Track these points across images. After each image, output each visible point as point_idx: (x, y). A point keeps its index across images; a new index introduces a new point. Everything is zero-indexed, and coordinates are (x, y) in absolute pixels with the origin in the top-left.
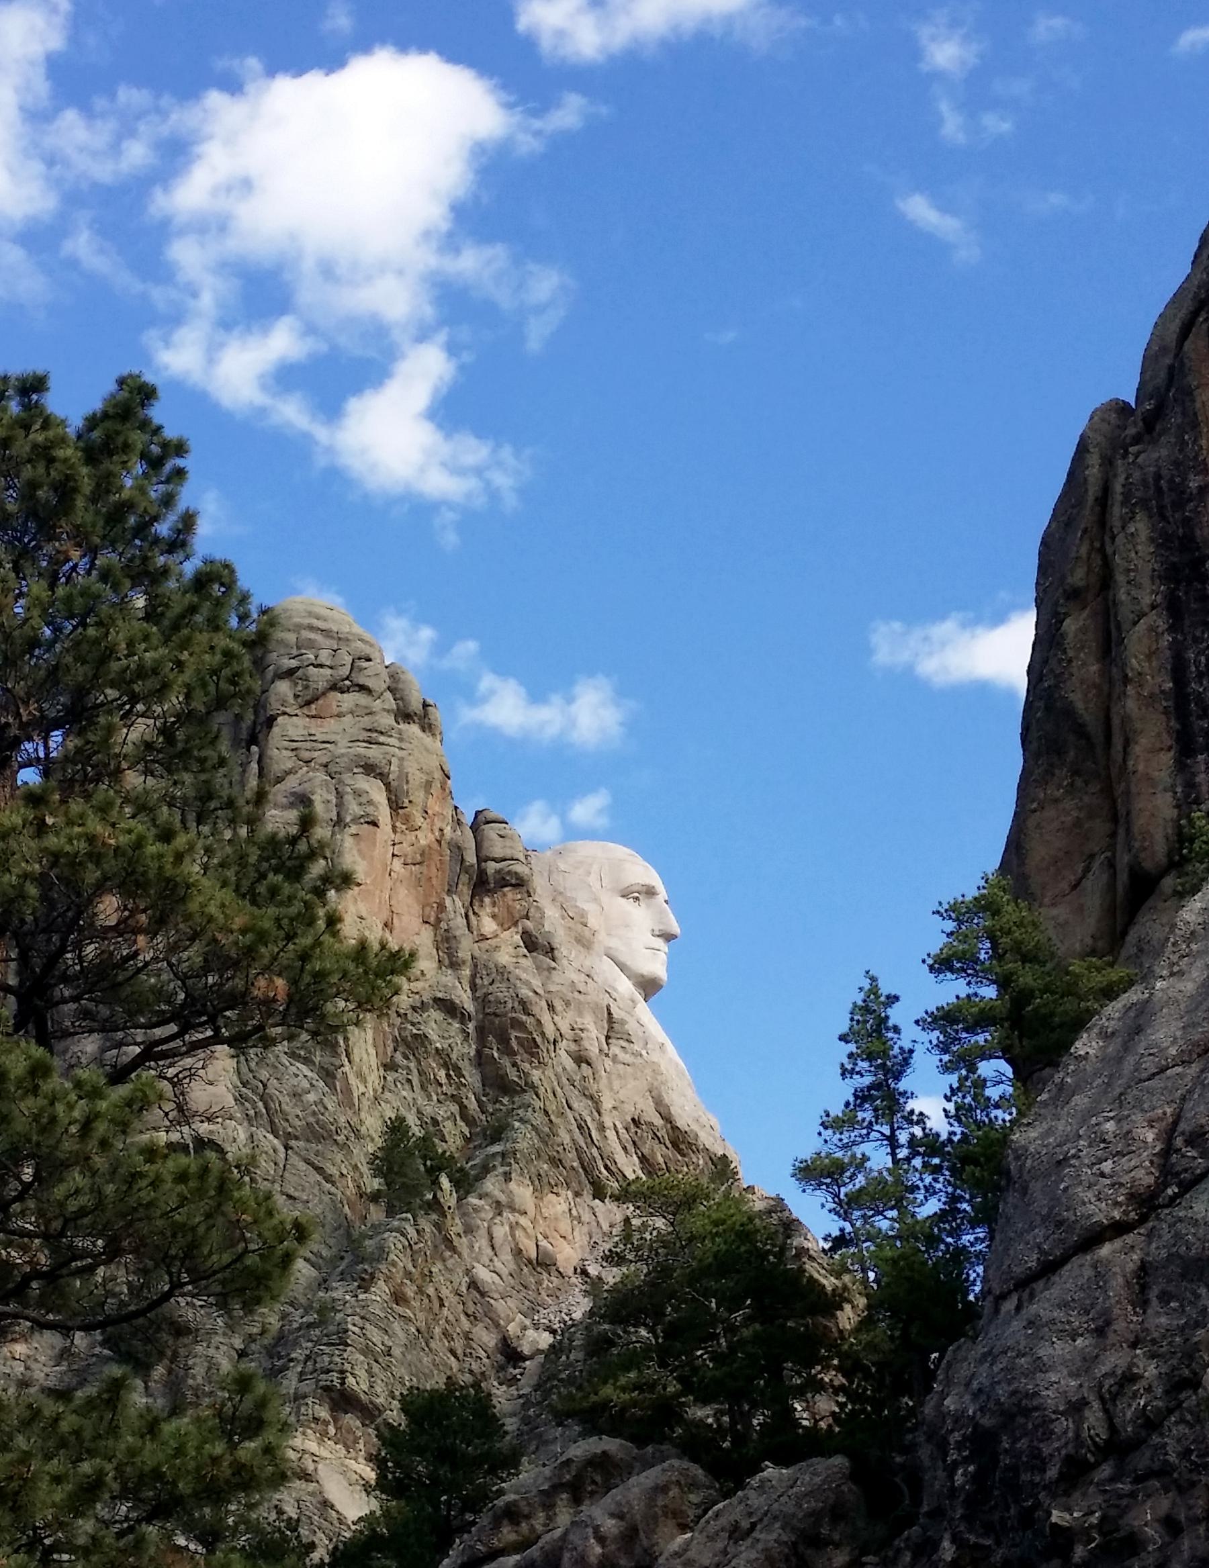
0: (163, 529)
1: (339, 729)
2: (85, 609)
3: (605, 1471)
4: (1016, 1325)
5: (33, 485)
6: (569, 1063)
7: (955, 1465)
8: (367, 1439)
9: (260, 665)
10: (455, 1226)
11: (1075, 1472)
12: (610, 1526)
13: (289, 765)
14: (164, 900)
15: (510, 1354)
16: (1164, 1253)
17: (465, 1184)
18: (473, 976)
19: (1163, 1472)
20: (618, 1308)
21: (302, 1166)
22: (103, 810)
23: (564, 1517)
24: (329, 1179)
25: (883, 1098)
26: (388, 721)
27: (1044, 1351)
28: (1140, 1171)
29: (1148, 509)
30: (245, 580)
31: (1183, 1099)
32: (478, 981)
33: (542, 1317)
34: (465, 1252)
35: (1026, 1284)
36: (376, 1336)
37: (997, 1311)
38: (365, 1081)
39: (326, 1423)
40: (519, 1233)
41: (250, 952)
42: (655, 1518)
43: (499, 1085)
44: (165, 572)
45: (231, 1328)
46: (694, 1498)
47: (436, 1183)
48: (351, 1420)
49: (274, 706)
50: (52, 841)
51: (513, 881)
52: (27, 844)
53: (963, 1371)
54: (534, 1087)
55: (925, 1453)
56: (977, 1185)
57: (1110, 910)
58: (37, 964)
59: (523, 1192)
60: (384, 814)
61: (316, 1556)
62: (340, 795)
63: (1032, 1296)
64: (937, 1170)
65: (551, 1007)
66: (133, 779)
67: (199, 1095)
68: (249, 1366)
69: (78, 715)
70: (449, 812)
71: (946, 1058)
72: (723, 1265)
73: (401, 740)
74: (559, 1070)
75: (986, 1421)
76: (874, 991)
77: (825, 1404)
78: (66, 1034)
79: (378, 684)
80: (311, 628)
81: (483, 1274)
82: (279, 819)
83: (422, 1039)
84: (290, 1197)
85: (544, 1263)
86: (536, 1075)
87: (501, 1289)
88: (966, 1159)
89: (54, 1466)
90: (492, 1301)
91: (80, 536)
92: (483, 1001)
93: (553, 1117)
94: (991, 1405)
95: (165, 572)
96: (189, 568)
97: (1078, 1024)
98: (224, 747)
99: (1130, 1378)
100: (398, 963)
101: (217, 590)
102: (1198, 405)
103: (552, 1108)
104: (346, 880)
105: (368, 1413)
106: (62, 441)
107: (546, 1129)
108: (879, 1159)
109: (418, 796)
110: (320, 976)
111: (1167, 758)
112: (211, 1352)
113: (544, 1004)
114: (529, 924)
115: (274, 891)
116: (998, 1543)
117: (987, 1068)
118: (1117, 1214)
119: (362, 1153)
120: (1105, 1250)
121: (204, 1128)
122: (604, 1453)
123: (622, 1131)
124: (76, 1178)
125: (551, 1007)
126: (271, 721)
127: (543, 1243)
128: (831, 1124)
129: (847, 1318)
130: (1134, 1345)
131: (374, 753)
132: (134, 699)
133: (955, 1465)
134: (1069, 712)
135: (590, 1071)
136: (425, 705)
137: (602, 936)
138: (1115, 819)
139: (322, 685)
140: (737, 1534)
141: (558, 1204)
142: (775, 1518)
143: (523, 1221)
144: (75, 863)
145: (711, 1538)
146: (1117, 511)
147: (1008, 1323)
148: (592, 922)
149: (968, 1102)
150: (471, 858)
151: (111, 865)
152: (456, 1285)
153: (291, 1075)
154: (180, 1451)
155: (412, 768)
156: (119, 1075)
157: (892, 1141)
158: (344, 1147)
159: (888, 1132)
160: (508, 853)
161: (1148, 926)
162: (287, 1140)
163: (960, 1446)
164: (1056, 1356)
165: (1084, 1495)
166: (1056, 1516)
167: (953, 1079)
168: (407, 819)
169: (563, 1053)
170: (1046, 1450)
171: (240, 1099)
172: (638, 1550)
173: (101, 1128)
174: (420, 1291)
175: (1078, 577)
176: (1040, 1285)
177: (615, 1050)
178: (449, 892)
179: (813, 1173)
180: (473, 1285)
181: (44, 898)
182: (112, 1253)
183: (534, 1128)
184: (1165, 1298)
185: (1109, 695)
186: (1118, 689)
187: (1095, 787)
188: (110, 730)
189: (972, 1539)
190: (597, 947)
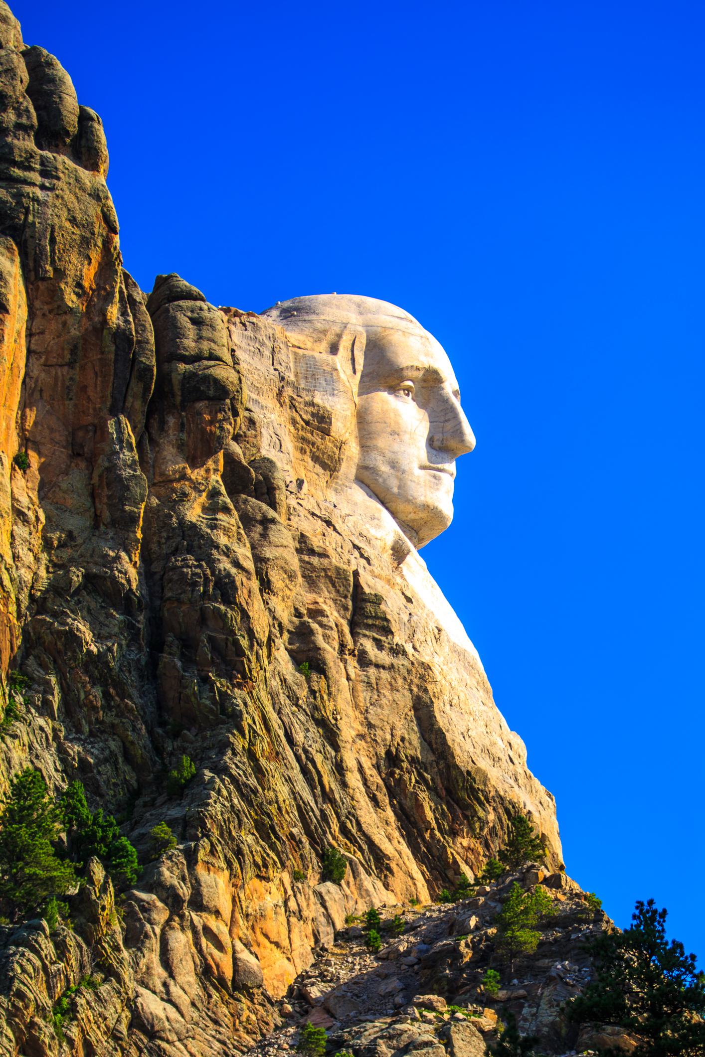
32: (154, 547)
34: (127, 974)
51: (211, 393)
73: (44, 174)
74: (275, 683)
87: (176, 1026)
90: (164, 1045)
93: (263, 762)
107: (253, 782)
113: (255, 584)
123: (370, 772)
125: (266, 586)
127: (244, 955)
135: (323, 683)
152: (111, 1023)
178: (114, 412)
183: (234, 780)
190: (348, 469)
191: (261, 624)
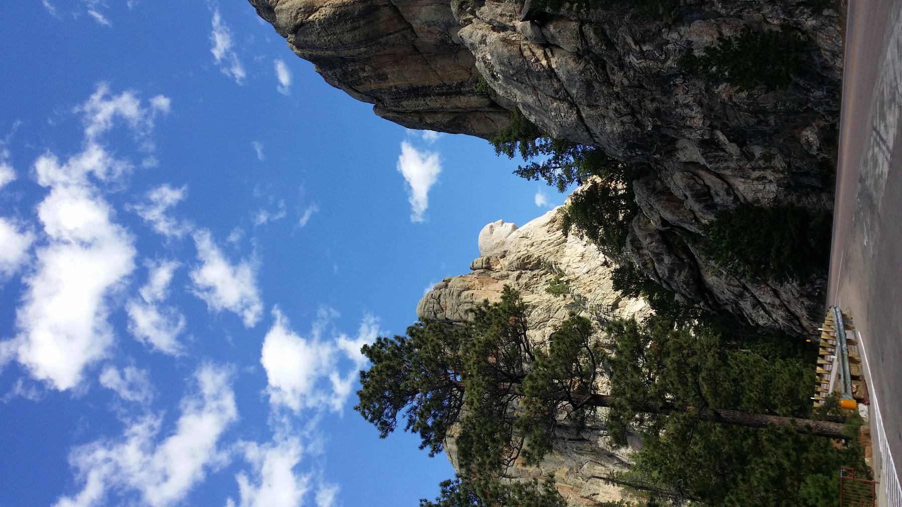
0: (399, 344)
2: (418, 364)
3: (635, 242)
5: (387, 375)
8: (625, 300)
9: (433, 321)
10: (572, 277)
14: (490, 346)
15: (605, 264)
17: (562, 274)
19: (639, 102)
20: (593, 236)
22: (467, 360)
25: (545, 170)
27: (609, 131)
28: (564, 106)
30: (412, 324)
33: (596, 256)
35: (591, 135)
41: (503, 325)
44: (409, 344)
45: (596, 332)
47: (562, 281)
48: (620, 304)
50: (475, 373)
52: (475, 379)
53: (612, 151)
55: (633, 161)
56: (566, 147)
58: (505, 377)
60: (471, 292)
61: (654, 313)
64: (562, 157)
66: (460, 353)
67: (538, 339)
68: (605, 329)
69: (444, 366)
72: (584, 210)
77: (620, 186)
78: (522, 371)
82: (471, 317)
85: (583, 256)
88: (560, 150)
89: (629, 377)
91: (400, 364)
95: (409, 344)
96: (409, 338)
97: (527, 121)
98: (452, 330)
99: (616, 110)
100: (507, 288)
101: (414, 331)
104: (486, 301)
105: (618, 300)
106: (376, 368)
108: (559, 171)
110: (510, 308)
115: (488, 319)
117: (537, 144)
119: (554, 299)
121: (547, 338)
124: (558, 370)
128: (550, 183)
129: (598, 180)
132: (440, 352)
141: (568, 251)
144: (480, 368)
149: (545, 149)
151: (481, 359)
153: (534, 316)
154: (626, 346)
156: (533, 358)
157: (555, 168)
161: (503, 104)
163: (631, 152)
164: (610, 128)
167: (540, 152)
173: (545, 363)
179: (562, 188)
181: (488, 375)
182: (577, 361)
188: (448, 358)
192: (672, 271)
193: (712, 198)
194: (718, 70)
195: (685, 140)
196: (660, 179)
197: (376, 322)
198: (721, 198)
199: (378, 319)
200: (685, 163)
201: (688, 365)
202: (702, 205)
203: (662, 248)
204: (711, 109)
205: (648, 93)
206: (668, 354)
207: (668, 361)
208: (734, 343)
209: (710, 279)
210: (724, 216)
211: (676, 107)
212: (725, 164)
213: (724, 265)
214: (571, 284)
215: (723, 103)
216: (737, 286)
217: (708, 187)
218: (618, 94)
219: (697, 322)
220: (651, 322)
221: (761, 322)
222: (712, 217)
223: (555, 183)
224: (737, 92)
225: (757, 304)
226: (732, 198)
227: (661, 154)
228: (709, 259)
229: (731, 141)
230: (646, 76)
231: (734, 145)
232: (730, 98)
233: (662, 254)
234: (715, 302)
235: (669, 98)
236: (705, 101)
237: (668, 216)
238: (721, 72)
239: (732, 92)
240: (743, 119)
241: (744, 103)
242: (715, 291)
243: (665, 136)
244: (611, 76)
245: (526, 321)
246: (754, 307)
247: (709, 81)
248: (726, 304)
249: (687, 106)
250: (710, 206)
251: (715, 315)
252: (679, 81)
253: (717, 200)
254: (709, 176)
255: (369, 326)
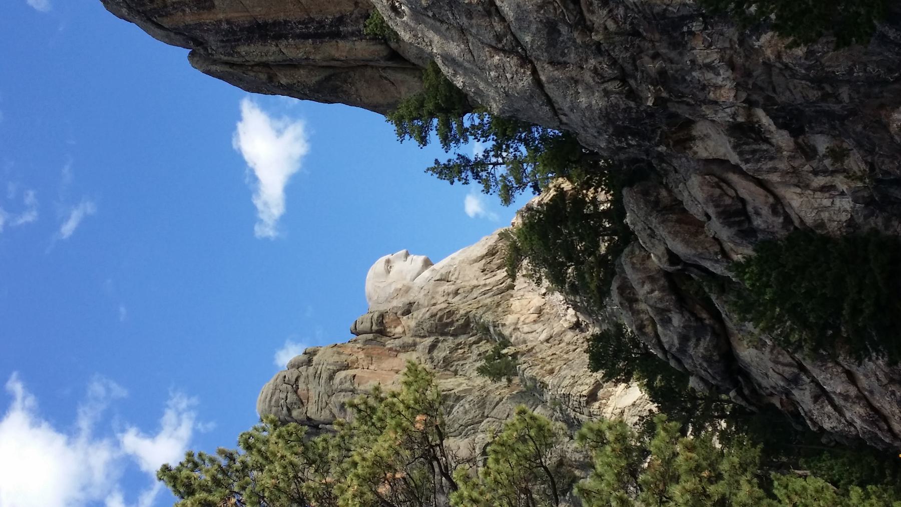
0: (224, 462)
1: (313, 390)
3: (626, 290)
4: (572, 116)
6: (458, 298)
7: (628, 144)
8: (608, 387)
10: (523, 348)
11: (632, 95)
12: (647, 287)
13: (328, 412)
15: (577, 326)
16: (545, 54)
17: (506, 343)
18: (420, 337)
19: (634, 59)
20: (558, 280)
21: (495, 410)
22: (343, 491)
23: (643, 306)
24: (501, 400)
26: (311, 370)
27: (584, 105)
28: (512, 62)
29: (236, 46)
31: (482, 43)
33: (562, 312)
34: (534, 344)
35: (555, 111)
36: (566, 382)
37: (566, 124)
38: (461, 384)
39: (601, 404)
40: (527, 321)
41: (404, 430)
42: (644, 268)
43: (465, 328)
46: (637, 253)
47: (505, 355)
48: (600, 393)
49: (303, 417)
53: (590, 139)
54: (467, 313)
55: (623, 156)
56: (515, 130)
57: (404, 69)
59: (510, 319)
60: (350, 372)
61: (655, 410)
62: (341, 391)
63: (561, 109)
64: (508, 147)
65: (434, 304)
67: (464, 453)
70: (350, 344)
71: (462, 140)
72: (543, 237)
75: (611, 130)
76: (433, 169)
77: (602, 197)
79: (295, 373)
80: (270, 401)
81: (543, 336)
83: (445, 359)
84: (508, 416)
85: (540, 311)
86: (462, 312)
88: (504, 134)
92: (431, 333)
94: (604, 128)
95: (243, 462)
96: (242, 451)
97: (450, 85)
99: (595, 71)
101: (252, 441)
102: (192, 23)
103: (476, 306)
104: (377, 389)
105: (598, 386)
108: (501, 170)
109: (343, 357)
110: (416, 401)
111: (341, 43)
112: (570, 450)
114: (399, 313)
115: (380, 420)
116: (659, 128)
117: (467, 124)
118: (529, 73)
119: (491, 385)
120: (543, 78)
121: (478, 451)
122: (618, 288)
123: (487, 277)
125: (434, 304)
126: (309, 419)
127: (531, 311)
128: (487, 190)
129: (567, 186)
130: (582, 68)
131: (325, 376)
133: (628, 144)
134: (320, 83)
136: (305, 353)
137: (405, 282)
138: (366, 66)
139: (295, 397)
140: (652, 235)
141: (516, 304)
142: (647, 219)
143: (522, 319)
145: (654, 246)
146: (235, 59)
147: (571, 120)
148: (399, 286)
149: (479, 132)
150: (371, 336)
153: (459, 413)
155: (331, 360)
156: (454, 487)
158: (488, 393)
159: (491, 166)
160: (369, 321)
161: (411, 55)
162: (484, 417)
163: (620, 142)
164: (586, 101)
165: (642, 91)
166: (650, 104)
167: (471, 138)
168: (353, 363)
169: (453, 300)
170: (623, 106)
171: (467, 436)
172: (657, 276)
173: (475, 494)
174: (549, 363)
175: (263, 77)
176: (556, 105)
177: (453, 278)
178: (384, 346)
179: (507, 198)
180: (547, 341)
184: (563, 54)
185: (313, 66)
186: (311, 62)
187: (352, 74)
189: (658, 138)
190: (411, 284)
191: (444, 306)
192: (684, 339)
193: (749, 219)
194: (760, 11)
195: (707, 123)
196: (666, 187)
197: (190, 408)
198: (764, 220)
199: (194, 401)
200: (707, 161)
201: (708, 497)
202: (733, 230)
203: (669, 301)
204: (748, 74)
205: (647, 45)
206: (676, 479)
207: (675, 490)
208: (784, 459)
209: (746, 353)
210: (768, 249)
211: (692, 69)
212: (770, 164)
213: (769, 329)
214: (521, 359)
215: (767, 65)
216: (789, 365)
217: (743, 201)
218: (598, 44)
219: (724, 425)
220: (649, 426)
221: (827, 425)
222: (749, 251)
223: (497, 190)
224: (789, 47)
225: (821, 394)
226: (781, 220)
227: (668, 146)
228: (744, 319)
229: (780, 126)
230: (645, 18)
231: (785, 133)
232: (779, 56)
233: (669, 311)
234: (753, 391)
235: (681, 54)
236: (739, 61)
237: (679, 248)
238: (763, 13)
239: (781, 46)
240: (797, 92)
241: (801, 66)
242: (755, 373)
243: (675, 116)
244: (587, 15)
245: (443, 424)
246: (816, 399)
247: (745, 27)
248: (772, 394)
249: (709, 67)
250: (747, 233)
251: (753, 413)
252: (696, 26)
253: (757, 222)
254: (744, 183)
255: (179, 414)
